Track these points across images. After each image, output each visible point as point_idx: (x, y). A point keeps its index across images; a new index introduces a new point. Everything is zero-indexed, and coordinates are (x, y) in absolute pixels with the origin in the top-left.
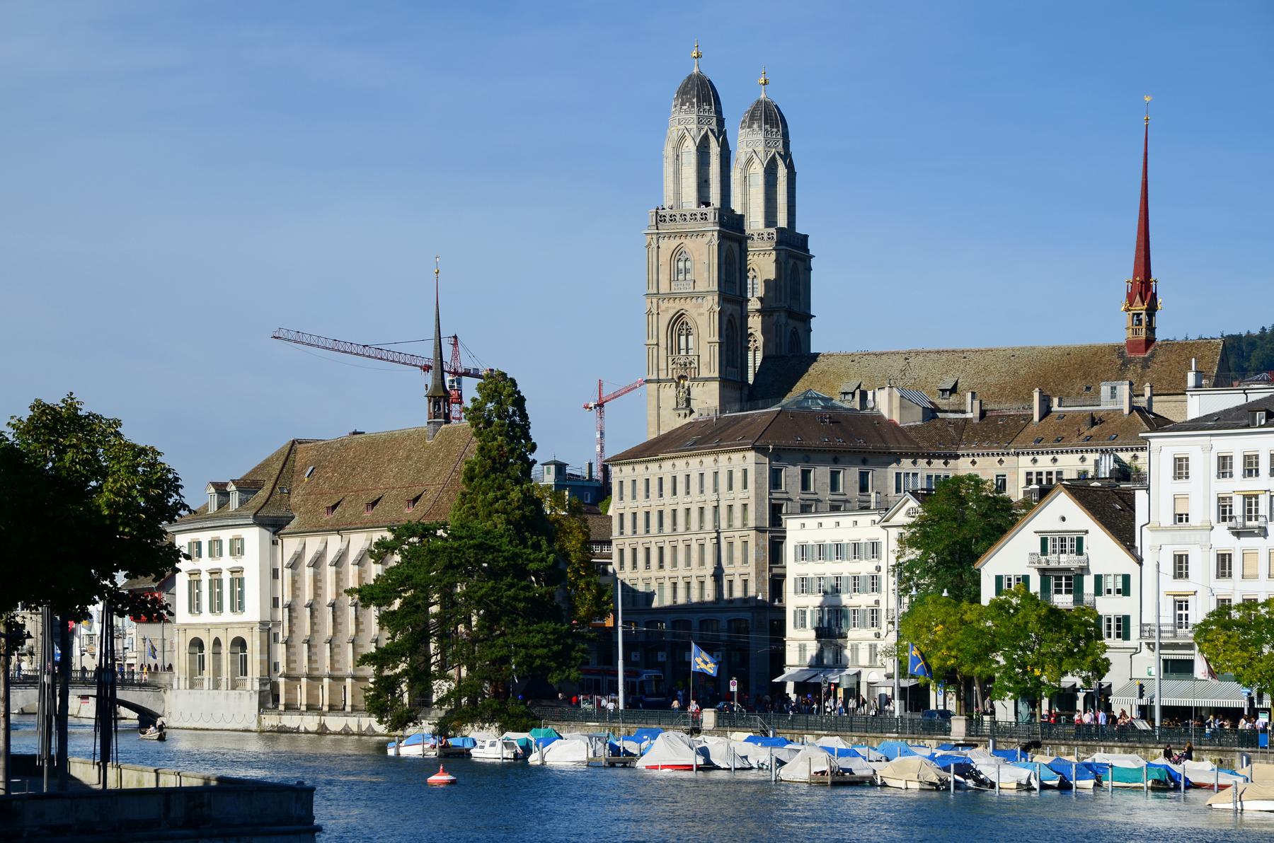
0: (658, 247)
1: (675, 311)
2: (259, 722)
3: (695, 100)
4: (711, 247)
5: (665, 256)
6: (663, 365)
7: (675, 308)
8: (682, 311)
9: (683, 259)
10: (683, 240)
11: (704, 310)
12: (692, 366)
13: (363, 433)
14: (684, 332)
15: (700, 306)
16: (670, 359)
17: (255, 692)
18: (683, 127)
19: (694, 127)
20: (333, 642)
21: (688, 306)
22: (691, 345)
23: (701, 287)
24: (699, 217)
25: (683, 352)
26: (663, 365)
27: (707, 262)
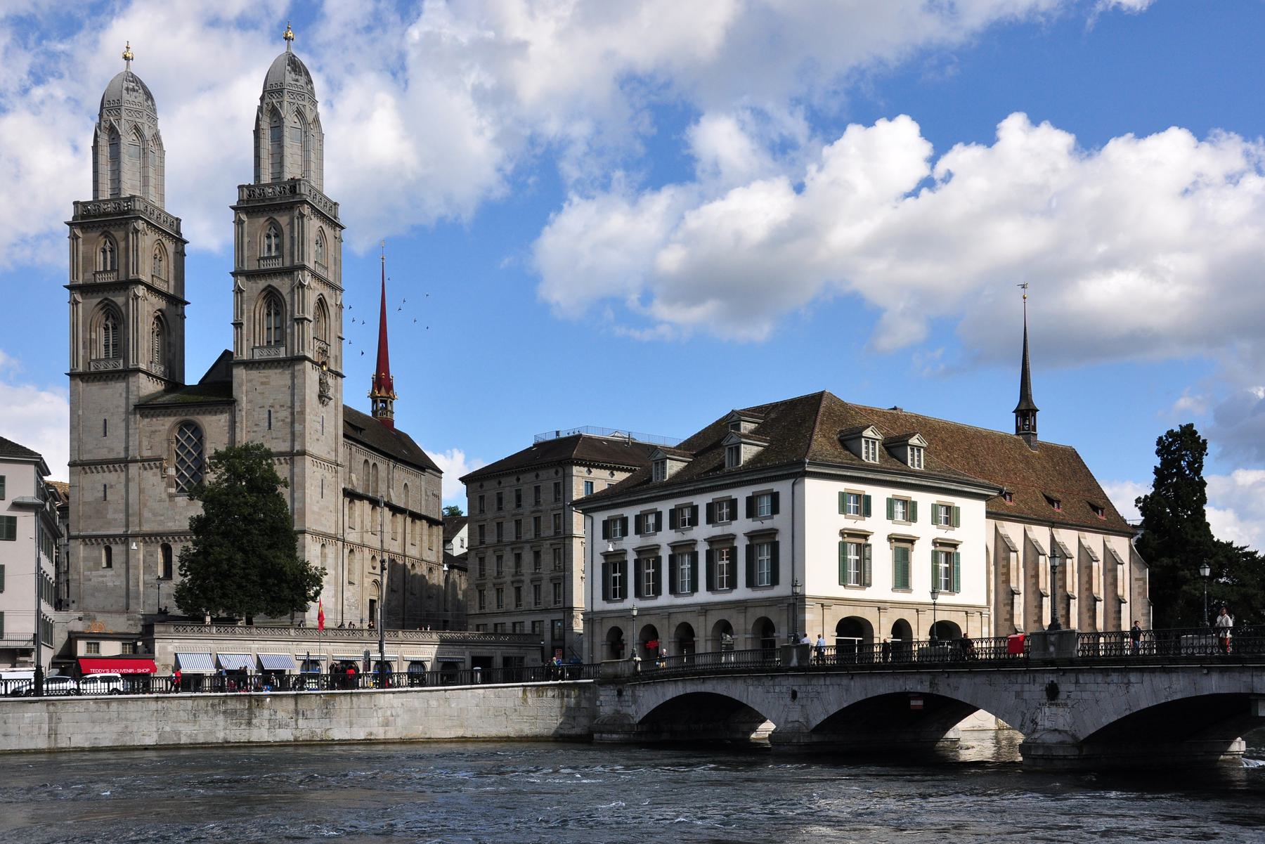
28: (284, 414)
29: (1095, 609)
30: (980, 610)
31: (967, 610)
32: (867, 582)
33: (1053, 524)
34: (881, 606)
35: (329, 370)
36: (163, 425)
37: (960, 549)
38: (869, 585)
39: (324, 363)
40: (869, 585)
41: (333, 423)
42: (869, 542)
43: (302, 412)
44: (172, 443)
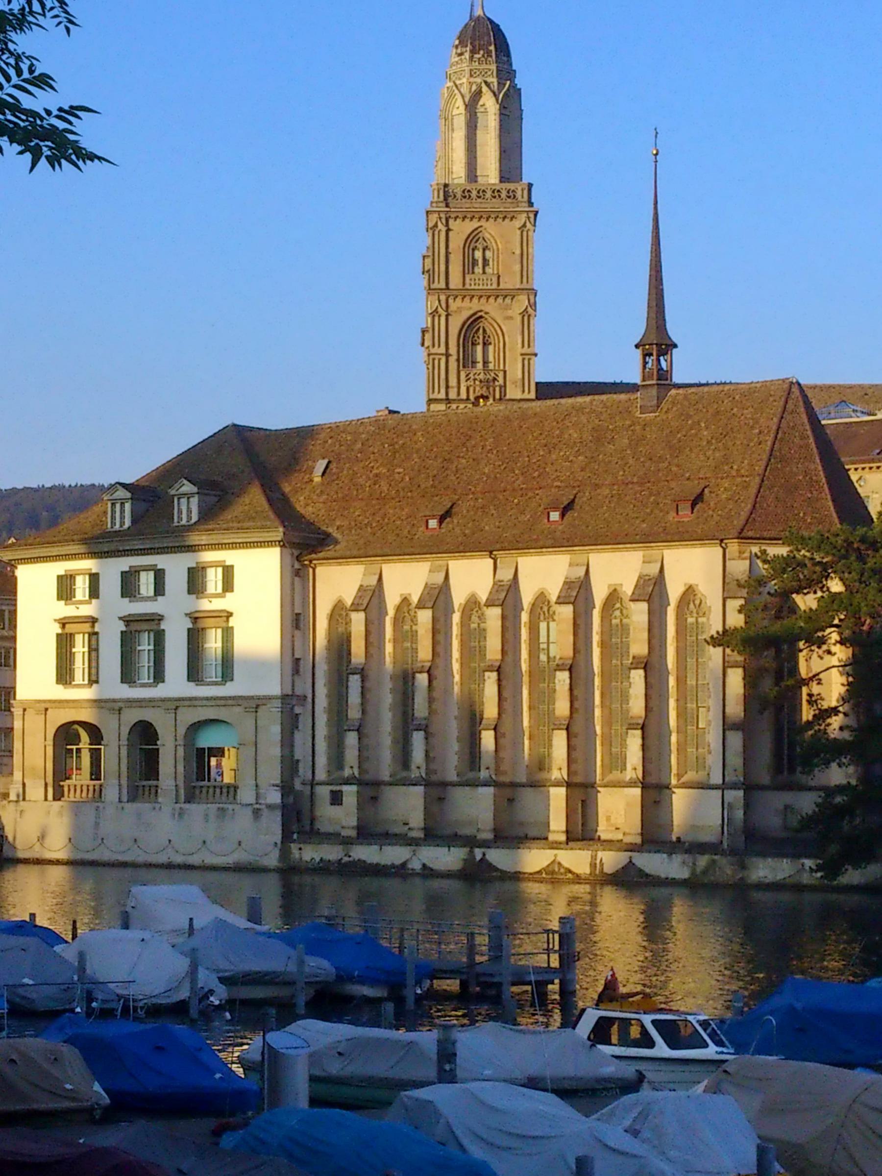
0: (448, 230)
3: (492, 48)
4: (525, 233)
5: (457, 241)
6: (453, 382)
7: (471, 308)
8: (480, 314)
9: (480, 247)
10: (483, 222)
12: (497, 383)
13: (398, 412)
14: (481, 341)
15: (508, 307)
16: (463, 375)
18: (479, 80)
19: (494, 80)
20: (498, 728)
21: (492, 308)
22: (491, 359)
24: (504, 194)
25: (480, 366)
26: (453, 382)
27: (518, 252)
39: (477, 399)
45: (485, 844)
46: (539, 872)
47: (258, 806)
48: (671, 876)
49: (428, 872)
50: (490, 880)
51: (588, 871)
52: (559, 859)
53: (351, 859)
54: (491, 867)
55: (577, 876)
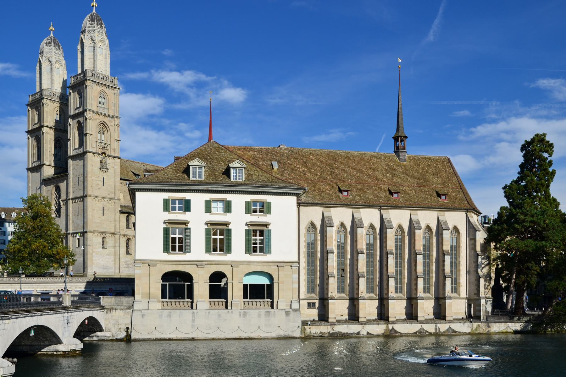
1: (99, 121)
2: (303, 331)
8: (103, 122)
9: (102, 97)
11: (113, 124)
15: (111, 122)
17: (295, 310)
21: (106, 120)
23: (111, 113)
28: (82, 178)
29: (416, 260)
30: (290, 264)
31: (278, 265)
32: (189, 250)
33: (380, 208)
34: (199, 264)
35: (108, 156)
36: (50, 188)
37: (270, 228)
38: (189, 252)
39: (102, 153)
40: (189, 252)
41: (113, 180)
42: (189, 227)
43: (87, 177)
44: (53, 195)
45: (393, 323)
46: (415, 333)
47: (286, 310)
48: (464, 331)
49: (370, 336)
50: (395, 337)
51: (434, 332)
52: (423, 327)
53: (335, 331)
54: (396, 332)
55: (430, 333)
